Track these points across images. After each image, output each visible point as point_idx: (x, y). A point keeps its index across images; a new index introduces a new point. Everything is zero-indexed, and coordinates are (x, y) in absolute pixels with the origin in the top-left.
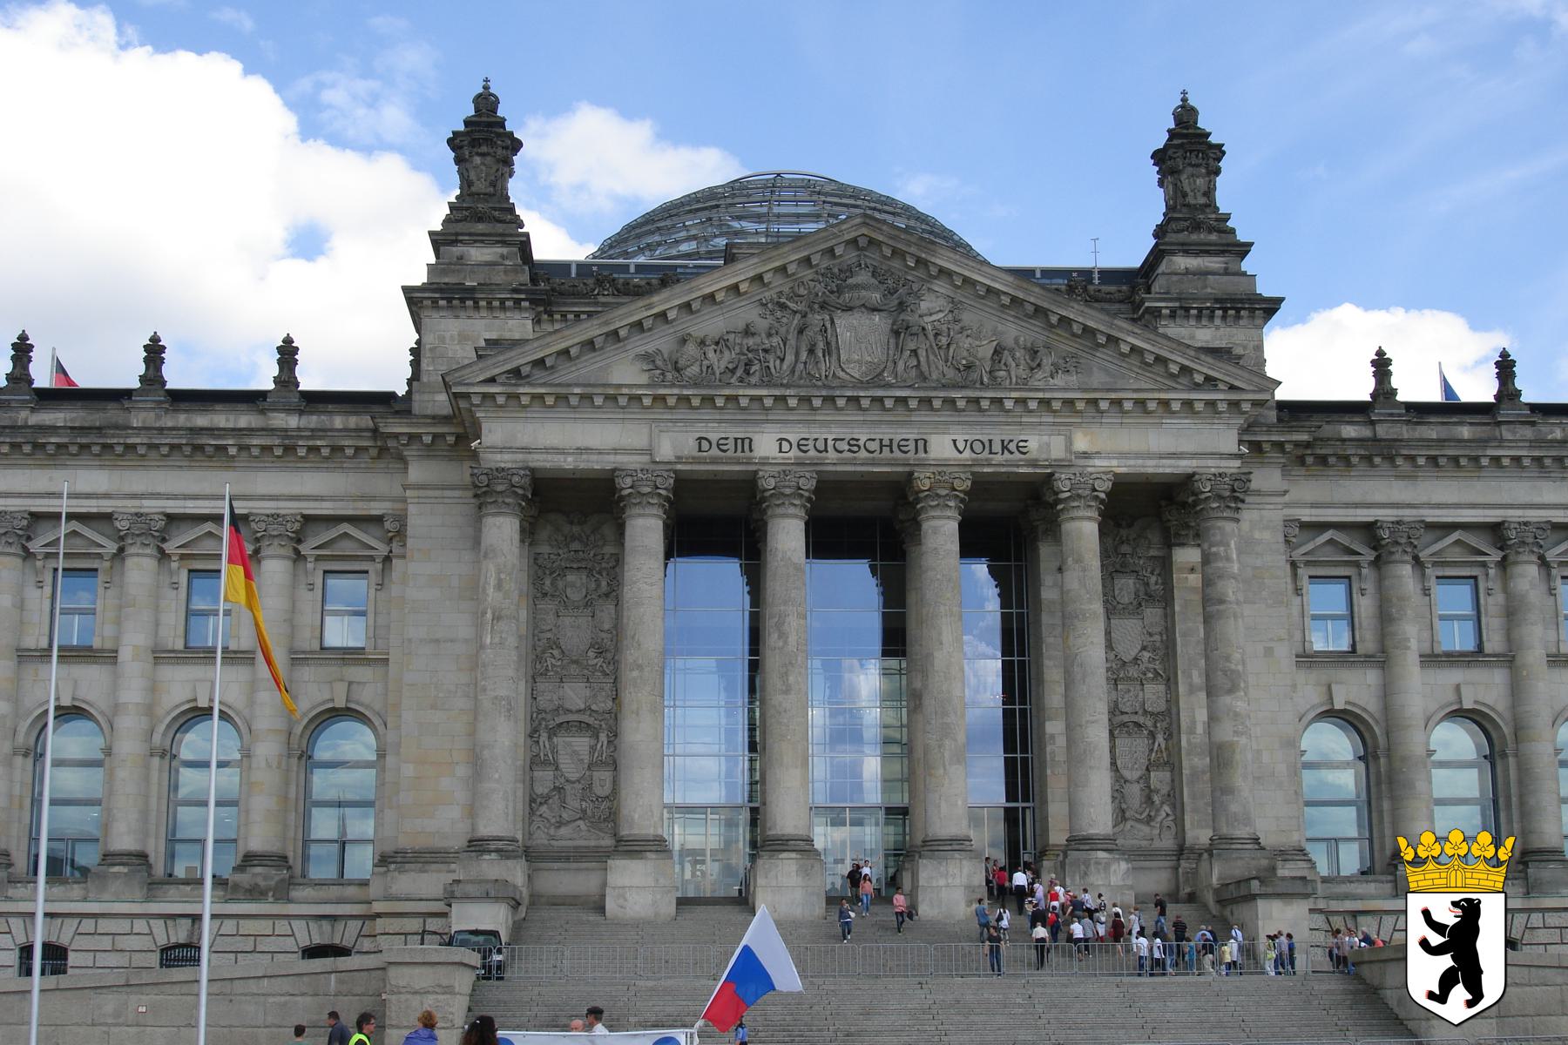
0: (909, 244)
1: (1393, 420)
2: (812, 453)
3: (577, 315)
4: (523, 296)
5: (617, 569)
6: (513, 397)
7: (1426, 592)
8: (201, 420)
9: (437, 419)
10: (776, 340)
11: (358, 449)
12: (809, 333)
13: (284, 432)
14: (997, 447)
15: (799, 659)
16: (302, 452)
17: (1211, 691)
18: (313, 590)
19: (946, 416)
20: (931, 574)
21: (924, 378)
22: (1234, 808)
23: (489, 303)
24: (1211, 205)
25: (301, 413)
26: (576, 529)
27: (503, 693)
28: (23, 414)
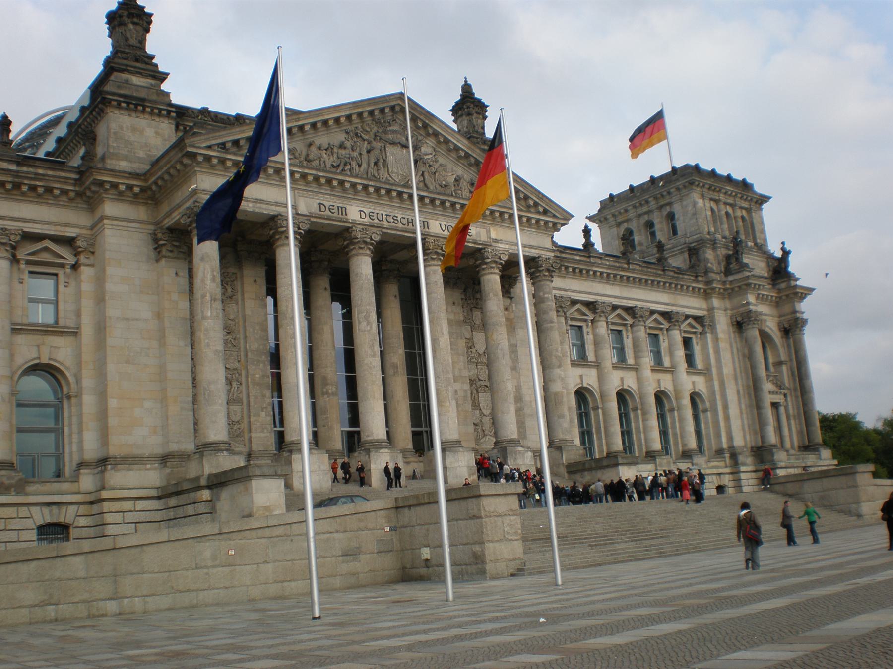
0: (421, 114)
2: (376, 221)
4: (173, 109)
5: (235, 283)
6: (222, 161)
7: (567, 330)
10: (355, 154)
11: (64, 192)
12: (376, 152)
16: (25, 189)
18: (22, 283)
19: (439, 210)
20: (433, 295)
23: (152, 111)
24: (484, 133)
25: (19, 164)
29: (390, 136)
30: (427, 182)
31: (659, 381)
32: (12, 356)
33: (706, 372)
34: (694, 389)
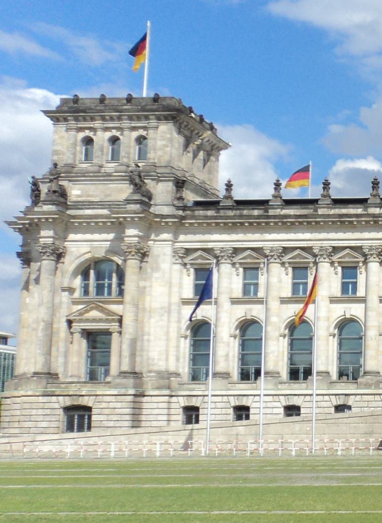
8: (344, 211)
28: (279, 210)
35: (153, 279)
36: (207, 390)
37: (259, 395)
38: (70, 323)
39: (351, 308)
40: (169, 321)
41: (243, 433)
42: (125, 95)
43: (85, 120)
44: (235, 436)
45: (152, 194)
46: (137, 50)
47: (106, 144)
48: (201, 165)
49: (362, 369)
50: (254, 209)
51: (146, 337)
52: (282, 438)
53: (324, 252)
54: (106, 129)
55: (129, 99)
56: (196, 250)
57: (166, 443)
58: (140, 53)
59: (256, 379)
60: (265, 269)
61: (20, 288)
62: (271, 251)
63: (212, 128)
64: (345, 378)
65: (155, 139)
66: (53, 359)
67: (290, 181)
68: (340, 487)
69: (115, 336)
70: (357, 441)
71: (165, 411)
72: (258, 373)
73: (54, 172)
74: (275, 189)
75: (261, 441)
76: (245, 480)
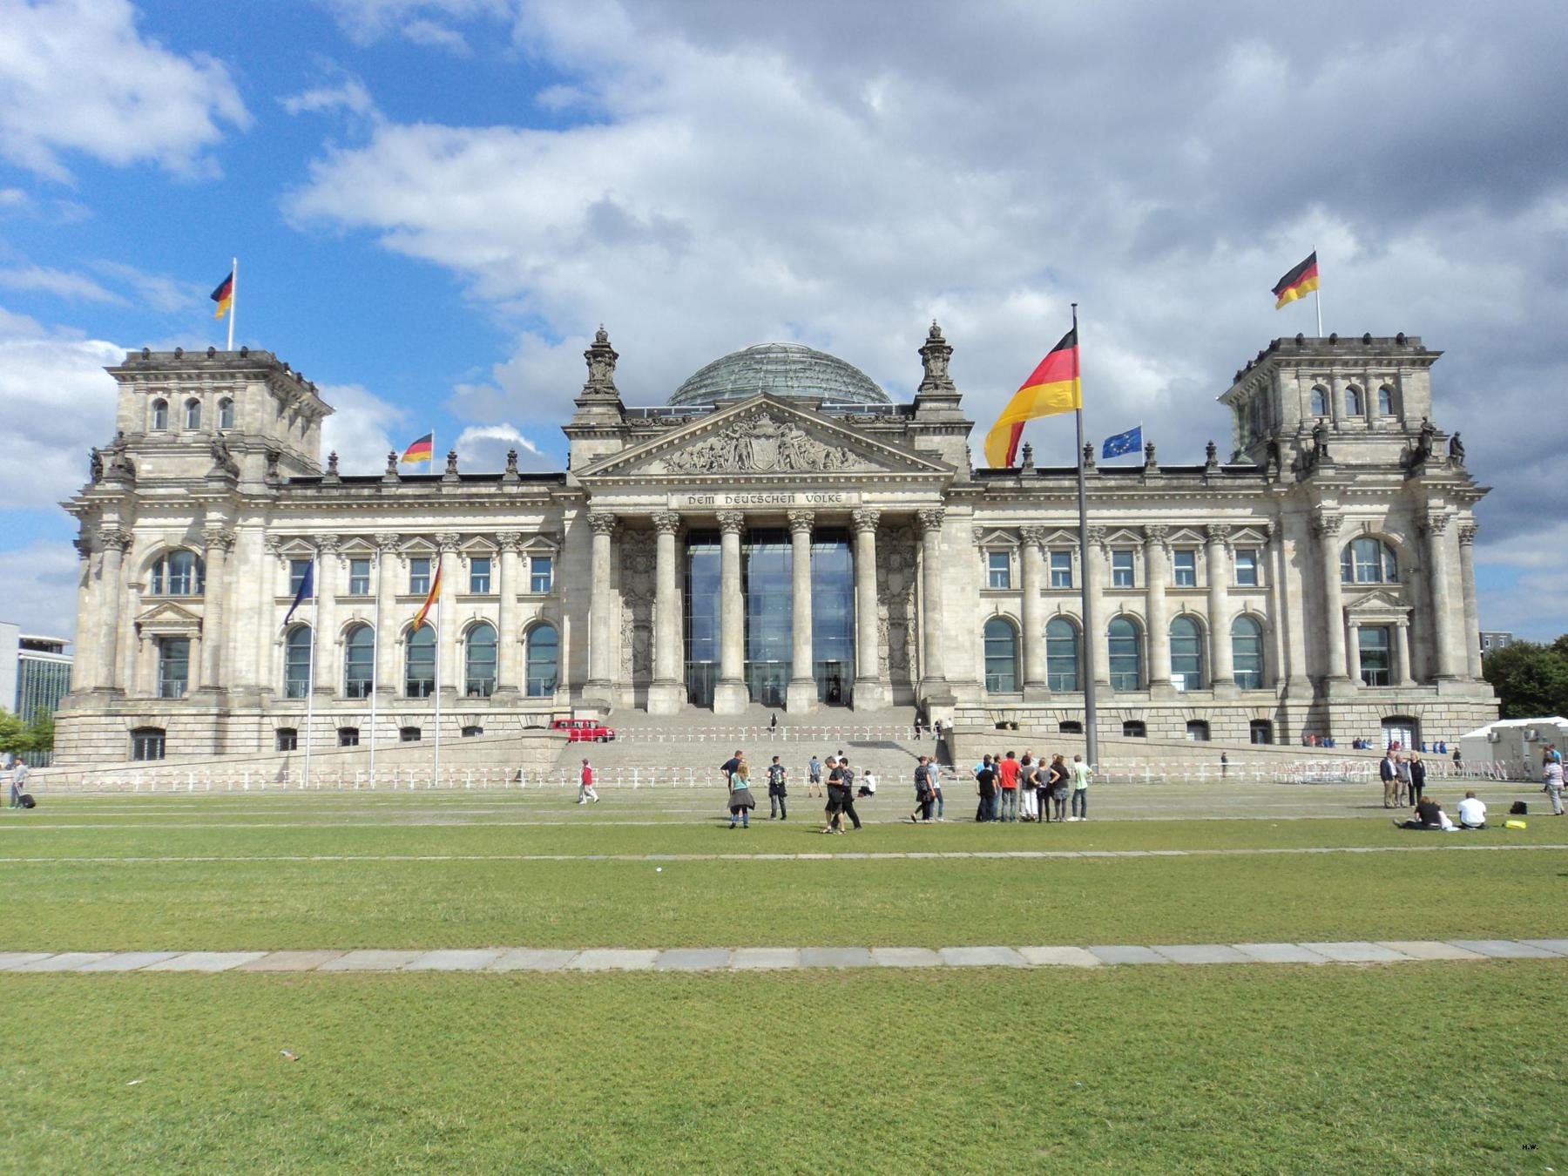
1: (1030, 478)
3: (643, 436)
6: (604, 482)
7: (1045, 560)
8: (474, 490)
9: (577, 489)
11: (543, 502)
13: (510, 496)
14: (827, 499)
15: (735, 597)
17: (925, 611)
21: (792, 467)
22: (933, 663)
25: (519, 486)
26: (641, 537)
27: (601, 615)
28: (394, 489)
29: (756, 432)
30: (793, 462)
31: (1183, 606)
32: (517, 616)
33: (1269, 592)
34: (1246, 610)
35: (241, 574)
36: (307, 708)
37: (370, 715)
38: (138, 626)
39: (481, 609)
40: (260, 625)
41: (350, 761)
42: (206, 349)
43: (157, 378)
44: (340, 766)
45: (239, 470)
46: (220, 294)
47: (183, 408)
48: (299, 433)
49: (496, 683)
50: (363, 488)
51: (231, 645)
52: (398, 767)
53: (449, 540)
54: (183, 390)
55: (211, 354)
56: (293, 537)
57: (257, 773)
58: (225, 297)
59: (366, 695)
60: (377, 560)
61: (79, 584)
62: (385, 539)
63: (312, 389)
64: (475, 694)
65: (243, 402)
66: (118, 671)
67: (408, 453)
68: (469, 828)
69: (194, 643)
70: (490, 772)
71: (255, 735)
72: (368, 688)
73: (119, 442)
74: (390, 463)
75: (373, 771)
76: (353, 818)
